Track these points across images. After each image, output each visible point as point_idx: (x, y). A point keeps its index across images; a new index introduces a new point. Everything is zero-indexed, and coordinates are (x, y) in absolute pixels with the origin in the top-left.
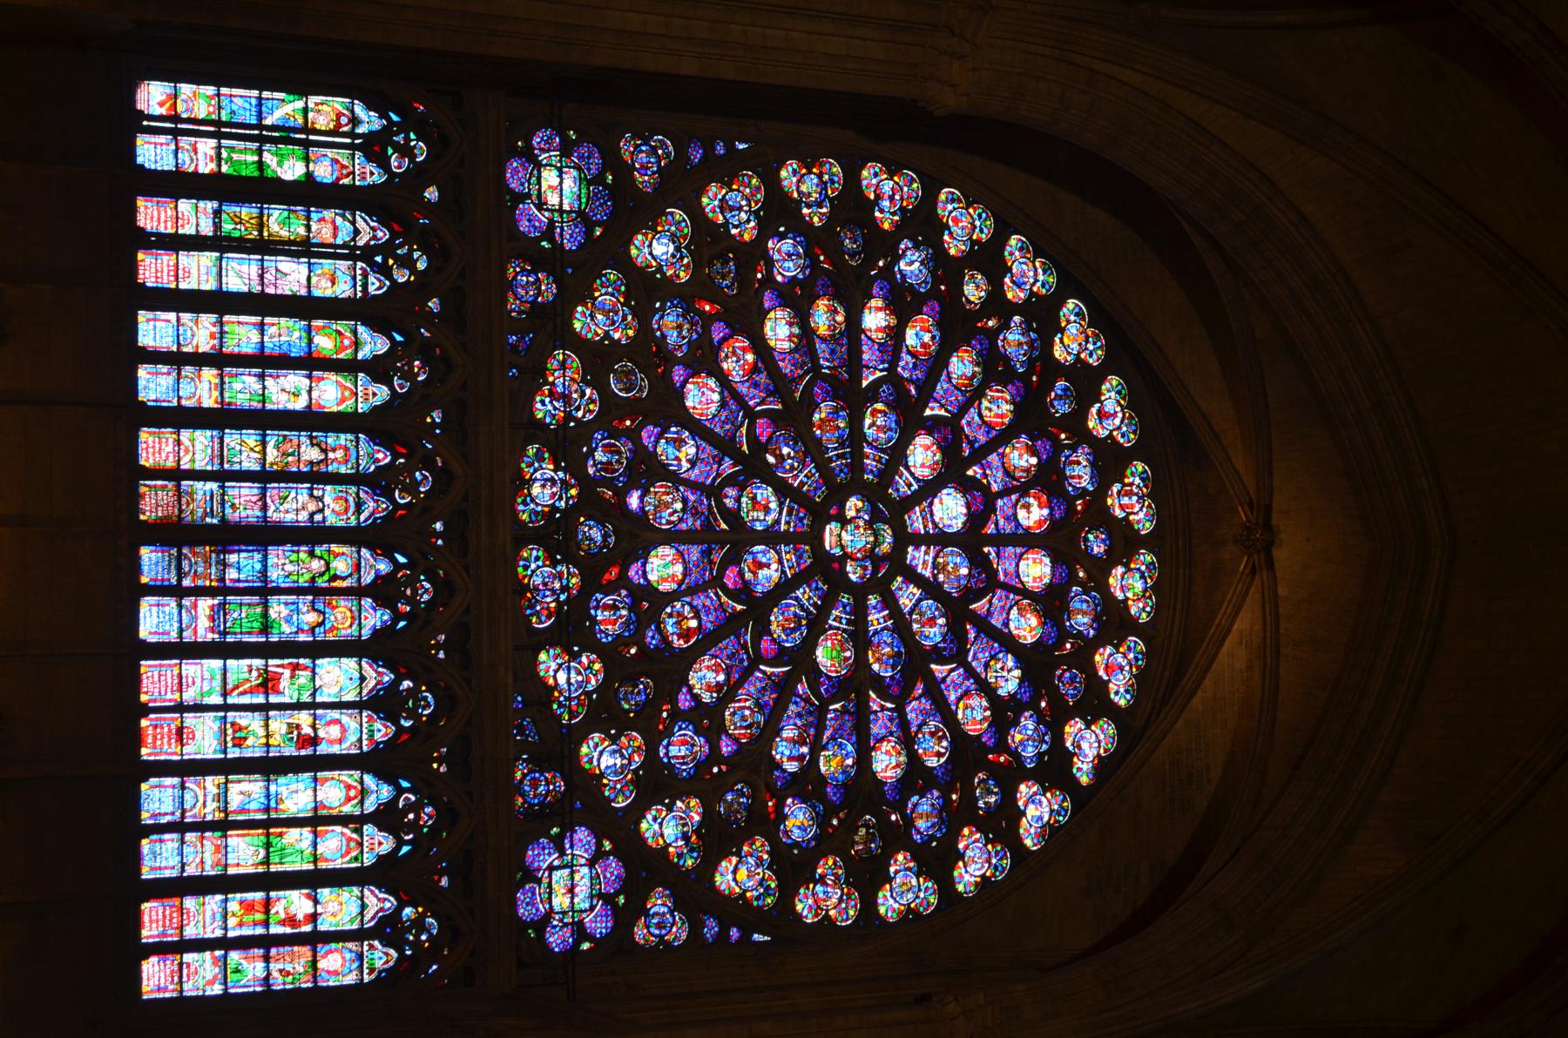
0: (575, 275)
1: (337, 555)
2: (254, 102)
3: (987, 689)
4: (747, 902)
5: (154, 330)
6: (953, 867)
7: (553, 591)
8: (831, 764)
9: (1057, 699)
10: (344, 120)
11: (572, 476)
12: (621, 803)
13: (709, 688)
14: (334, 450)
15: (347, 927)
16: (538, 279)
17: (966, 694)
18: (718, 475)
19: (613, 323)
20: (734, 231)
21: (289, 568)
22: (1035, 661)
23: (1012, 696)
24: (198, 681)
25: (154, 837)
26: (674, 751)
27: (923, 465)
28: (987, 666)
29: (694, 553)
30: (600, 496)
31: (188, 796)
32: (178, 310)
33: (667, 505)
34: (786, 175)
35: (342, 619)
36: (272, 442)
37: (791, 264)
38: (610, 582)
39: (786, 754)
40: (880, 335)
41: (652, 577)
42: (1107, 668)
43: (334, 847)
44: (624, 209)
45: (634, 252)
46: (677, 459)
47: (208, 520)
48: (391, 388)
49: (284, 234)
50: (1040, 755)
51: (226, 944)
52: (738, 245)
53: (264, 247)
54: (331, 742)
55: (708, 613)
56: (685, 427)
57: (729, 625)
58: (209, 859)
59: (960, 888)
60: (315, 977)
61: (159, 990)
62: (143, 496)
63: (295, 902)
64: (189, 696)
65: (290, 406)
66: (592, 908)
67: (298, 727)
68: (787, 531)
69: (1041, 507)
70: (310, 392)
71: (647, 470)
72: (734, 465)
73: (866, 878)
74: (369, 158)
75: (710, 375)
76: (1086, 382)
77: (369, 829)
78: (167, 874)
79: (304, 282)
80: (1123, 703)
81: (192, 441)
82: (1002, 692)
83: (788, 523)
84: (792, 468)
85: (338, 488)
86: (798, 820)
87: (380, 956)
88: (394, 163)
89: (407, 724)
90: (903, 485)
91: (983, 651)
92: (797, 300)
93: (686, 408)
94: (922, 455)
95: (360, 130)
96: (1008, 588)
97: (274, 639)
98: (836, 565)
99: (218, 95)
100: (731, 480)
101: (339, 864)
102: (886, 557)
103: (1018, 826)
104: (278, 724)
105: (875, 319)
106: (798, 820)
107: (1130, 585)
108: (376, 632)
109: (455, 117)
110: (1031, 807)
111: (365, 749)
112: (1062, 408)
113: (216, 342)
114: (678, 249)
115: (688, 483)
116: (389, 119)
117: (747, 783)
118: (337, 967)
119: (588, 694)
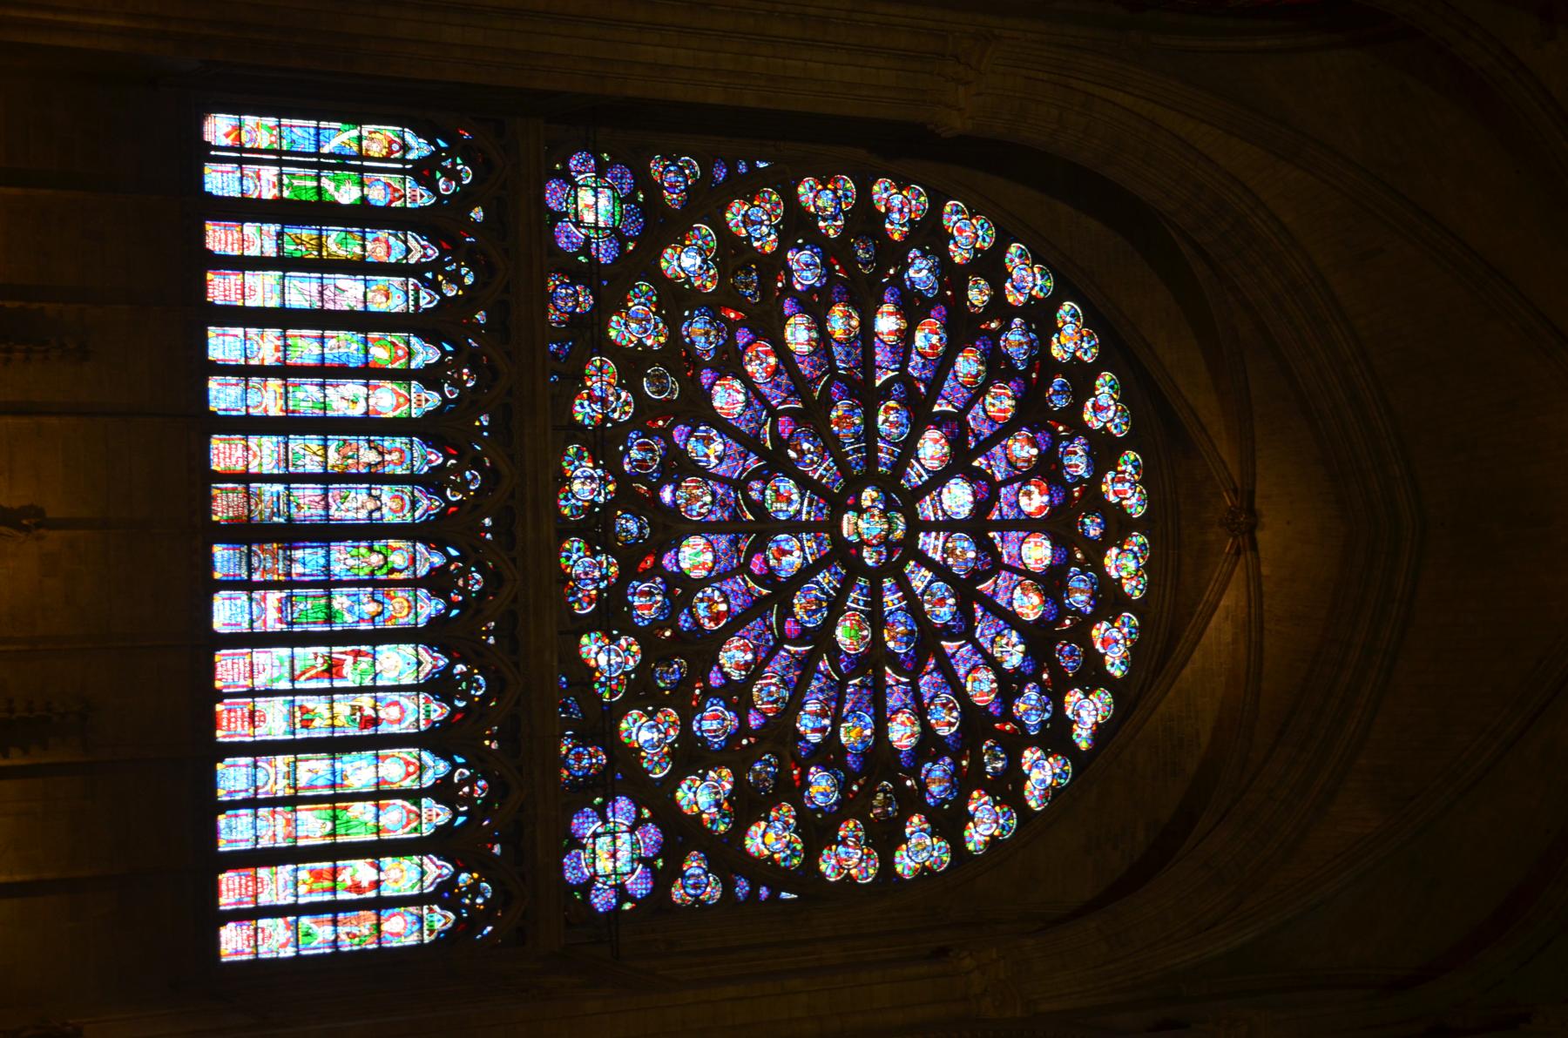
1: (394, 549)
2: (312, 131)
3: (993, 663)
4: (776, 863)
5: (223, 345)
6: (964, 827)
7: (593, 580)
8: (849, 735)
10: (395, 147)
12: (658, 774)
13: (738, 667)
14: (390, 453)
15: (409, 893)
16: (576, 292)
17: (975, 668)
18: (744, 470)
19: (646, 330)
20: (756, 244)
21: (351, 562)
22: (1037, 636)
23: (1017, 670)
24: (268, 667)
25: (230, 812)
26: (706, 725)
27: (932, 458)
28: (993, 642)
29: (723, 542)
30: (636, 492)
31: (261, 775)
32: (244, 326)
33: (698, 498)
35: (403, 609)
36: (333, 445)
38: (645, 570)
39: (808, 725)
42: (1104, 642)
43: (396, 820)
44: (656, 225)
45: (664, 265)
46: (706, 455)
47: (275, 519)
48: (442, 394)
49: (342, 253)
50: (1043, 723)
51: (296, 910)
52: (760, 257)
53: (325, 265)
54: (391, 722)
55: (736, 597)
56: (712, 425)
57: (757, 608)
58: (281, 831)
60: (379, 938)
61: (237, 953)
62: (215, 498)
63: (359, 871)
64: (260, 682)
65: (350, 413)
66: (633, 871)
67: (361, 709)
68: (808, 521)
69: (1041, 494)
70: (367, 399)
71: (679, 467)
72: (759, 460)
73: (885, 838)
74: (419, 182)
75: (735, 377)
76: (1081, 378)
77: (425, 802)
78: (242, 846)
79: (361, 297)
80: (1118, 674)
81: (260, 446)
82: (1006, 666)
83: (809, 513)
84: (813, 463)
85: (395, 487)
86: (821, 787)
87: (439, 919)
88: (442, 185)
89: (461, 704)
91: (990, 628)
92: (815, 306)
93: (713, 409)
94: (932, 448)
95: (410, 156)
96: (1012, 569)
97: (337, 628)
98: (853, 552)
99: (280, 126)
100: (756, 475)
101: (400, 834)
102: (899, 542)
103: (1023, 789)
104: (343, 706)
105: (887, 324)
106: (821, 787)
107: (1123, 565)
108: (431, 620)
110: (1035, 771)
111: (423, 728)
112: (1060, 403)
114: (704, 261)
115: (715, 477)
116: (437, 145)
117: (775, 754)
118: (400, 929)
119: (627, 674)
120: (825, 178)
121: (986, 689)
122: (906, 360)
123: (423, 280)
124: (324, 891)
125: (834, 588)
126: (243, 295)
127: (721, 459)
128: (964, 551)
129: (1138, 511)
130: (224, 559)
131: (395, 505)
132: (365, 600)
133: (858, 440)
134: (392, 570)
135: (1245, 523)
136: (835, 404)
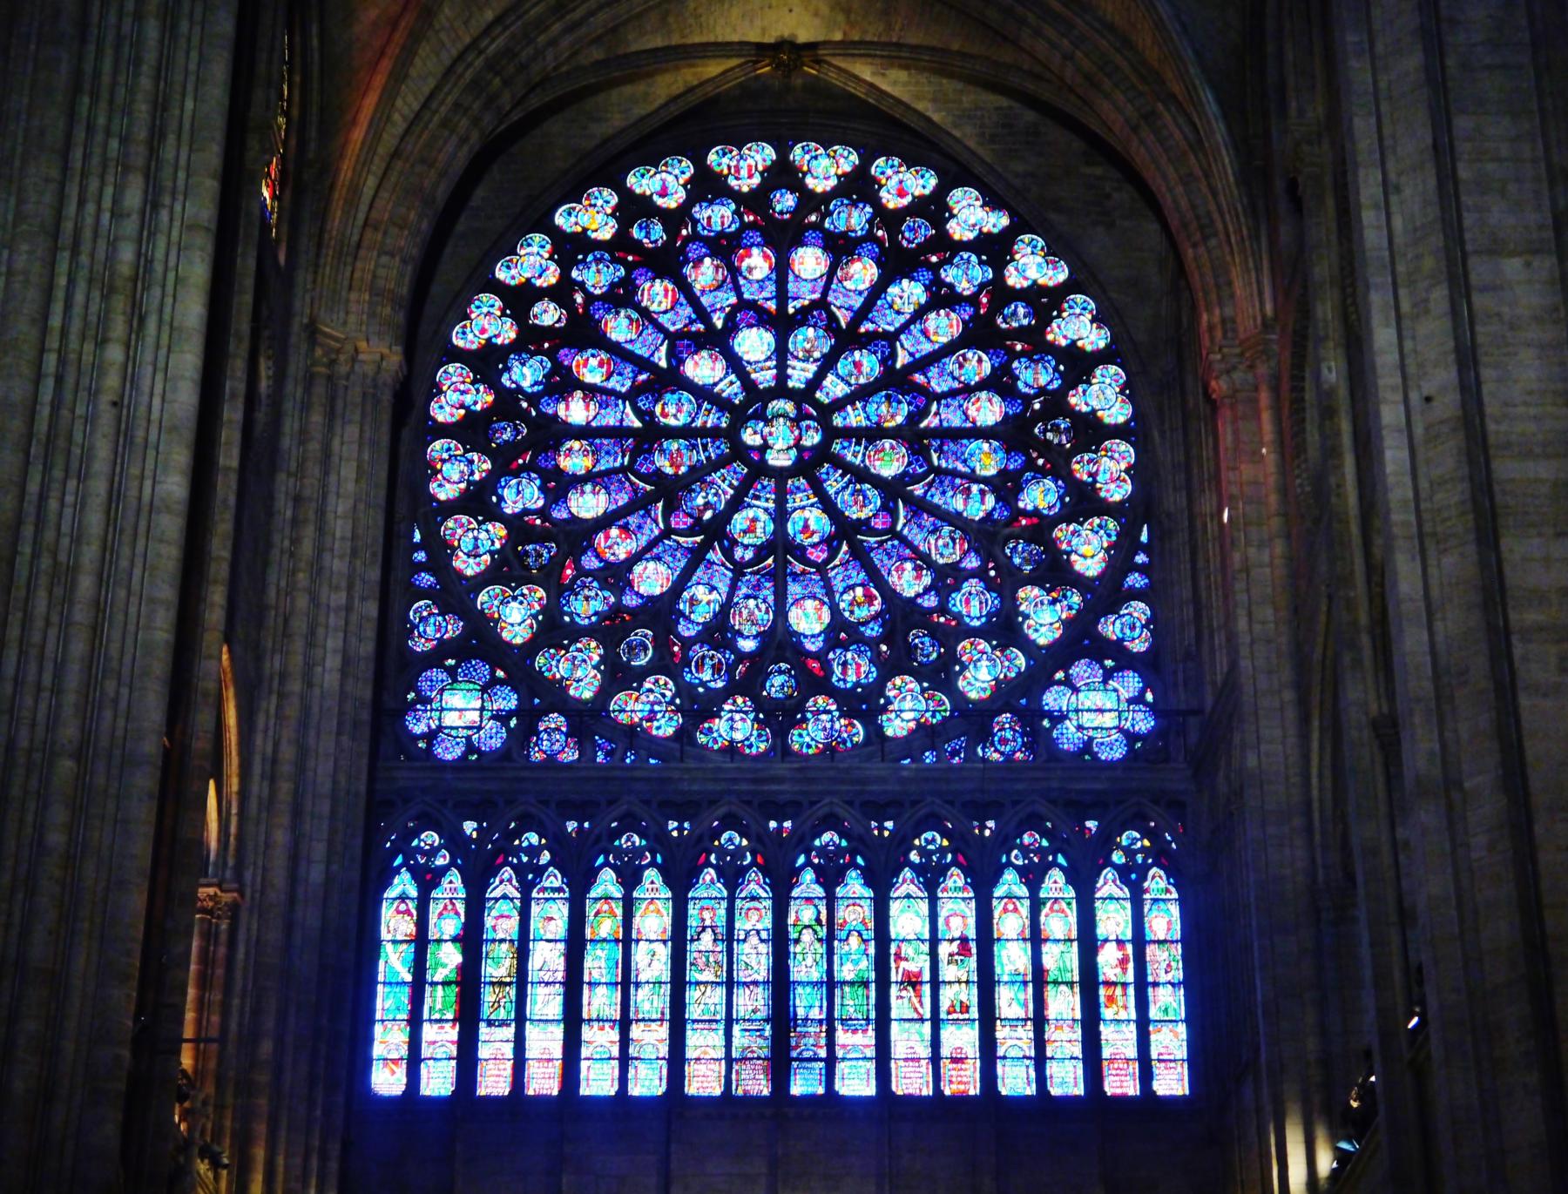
0: (539, 696)
1: (798, 919)
2: (388, 989)
4: (1111, 546)
5: (598, 1081)
6: (1082, 350)
9: (930, 245)
10: (403, 907)
11: (725, 702)
12: (1021, 661)
17: (925, 333)
20: (497, 545)
21: (809, 961)
22: (895, 265)
23: (927, 288)
27: (713, 369)
28: (898, 313)
29: (794, 589)
30: (744, 675)
31: (1011, 1053)
33: (751, 614)
34: (445, 492)
37: (527, 492)
38: (822, 668)
39: (978, 506)
40: (592, 406)
41: (817, 628)
43: (1060, 923)
45: (518, 641)
46: (708, 603)
47: (768, 1033)
49: (507, 963)
50: (981, 263)
51: (1143, 1025)
53: (522, 978)
54: (965, 925)
55: (850, 577)
56: (679, 596)
57: (860, 556)
58: (1065, 1034)
59: (1102, 344)
64: (925, 1052)
66: (1115, 690)
67: (951, 955)
68: (775, 501)
69: (749, 255)
71: (719, 631)
73: (1091, 432)
74: (437, 884)
75: (630, 571)
76: (633, 208)
77: (1042, 895)
78: (1080, 1072)
81: (696, 1047)
82: (923, 300)
84: (716, 494)
85: (737, 916)
86: (1040, 496)
88: (440, 862)
89: (949, 857)
90: (731, 388)
92: (559, 486)
94: (703, 368)
96: (826, 289)
97: (872, 976)
100: (728, 553)
101: (1073, 918)
102: (798, 408)
104: (948, 972)
105: (576, 411)
106: (1040, 496)
108: (868, 883)
109: (399, 802)
112: (658, 231)
113: (607, 1025)
114: (515, 598)
115: (731, 595)
116: (401, 866)
119: (923, 691)
120: (430, 471)
121: (943, 321)
122: (612, 393)
123: (533, 884)
124: (1125, 994)
125: (843, 476)
126: (549, 1060)
127: (713, 589)
128: (807, 340)
130: (804, 1084)
131: (754, 916)
132: (846, 948)
133: (694, 447)
134: (818, 920)
135: (786, 52)
136: (658, 470)
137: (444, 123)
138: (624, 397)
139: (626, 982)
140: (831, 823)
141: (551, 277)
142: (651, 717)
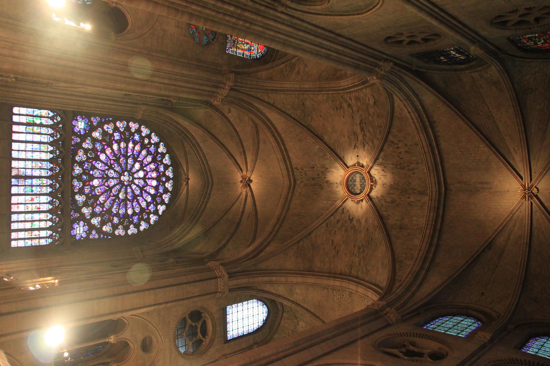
0: (83, 138)
5: (15, 146)
9: (157, 202)
12: (88, 218)
22: (154, 197)
29: (101, 180)
39: (114, 210)
44: (91, 128)
51: (24, 239)
52: (110, 134)
57: (106, 191)
71: (94, 168)
73: (126, 228)
76: (163, 155)
87: (50, 241)
92: (119, 142)
94: (137, 166)
100: (107, 169)
104: (34, 206)
105: (131, 145)
106: (116, 220)
107: (169, 185)
120: (121, 121)
129: (171, 177)
130: (14, 181)
137: (177, 127)
138: (133, 153)
139: (33, 151)
140: (60, 186)
141: (152, 142)
142: (79, 156)
